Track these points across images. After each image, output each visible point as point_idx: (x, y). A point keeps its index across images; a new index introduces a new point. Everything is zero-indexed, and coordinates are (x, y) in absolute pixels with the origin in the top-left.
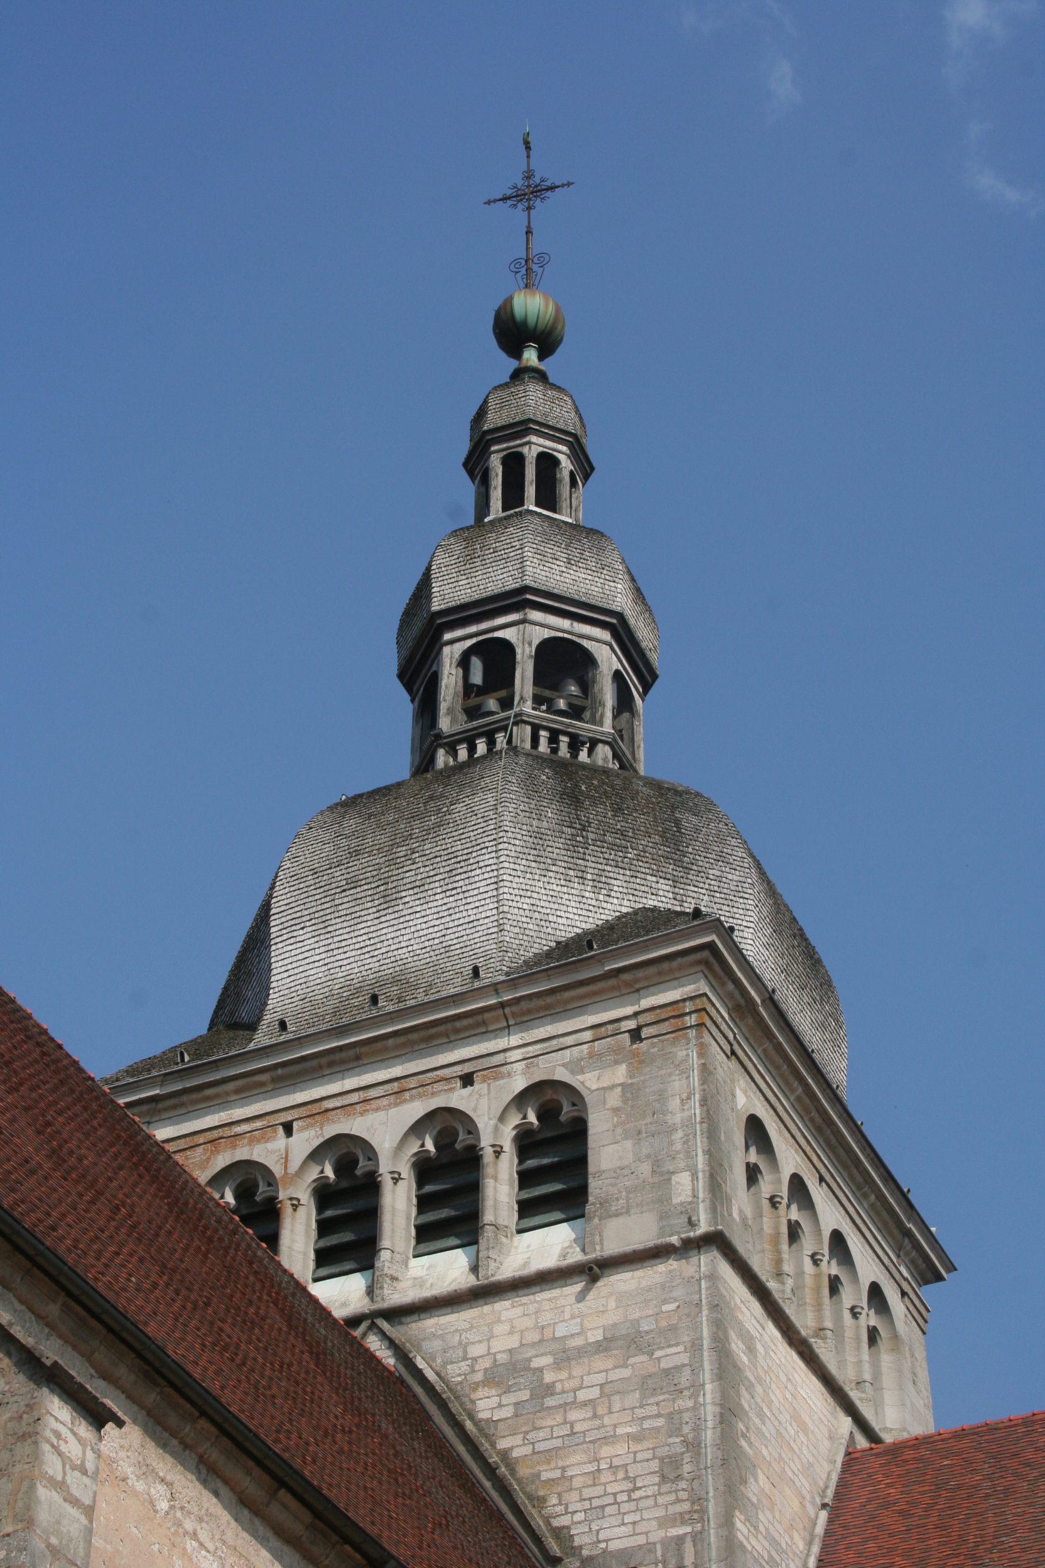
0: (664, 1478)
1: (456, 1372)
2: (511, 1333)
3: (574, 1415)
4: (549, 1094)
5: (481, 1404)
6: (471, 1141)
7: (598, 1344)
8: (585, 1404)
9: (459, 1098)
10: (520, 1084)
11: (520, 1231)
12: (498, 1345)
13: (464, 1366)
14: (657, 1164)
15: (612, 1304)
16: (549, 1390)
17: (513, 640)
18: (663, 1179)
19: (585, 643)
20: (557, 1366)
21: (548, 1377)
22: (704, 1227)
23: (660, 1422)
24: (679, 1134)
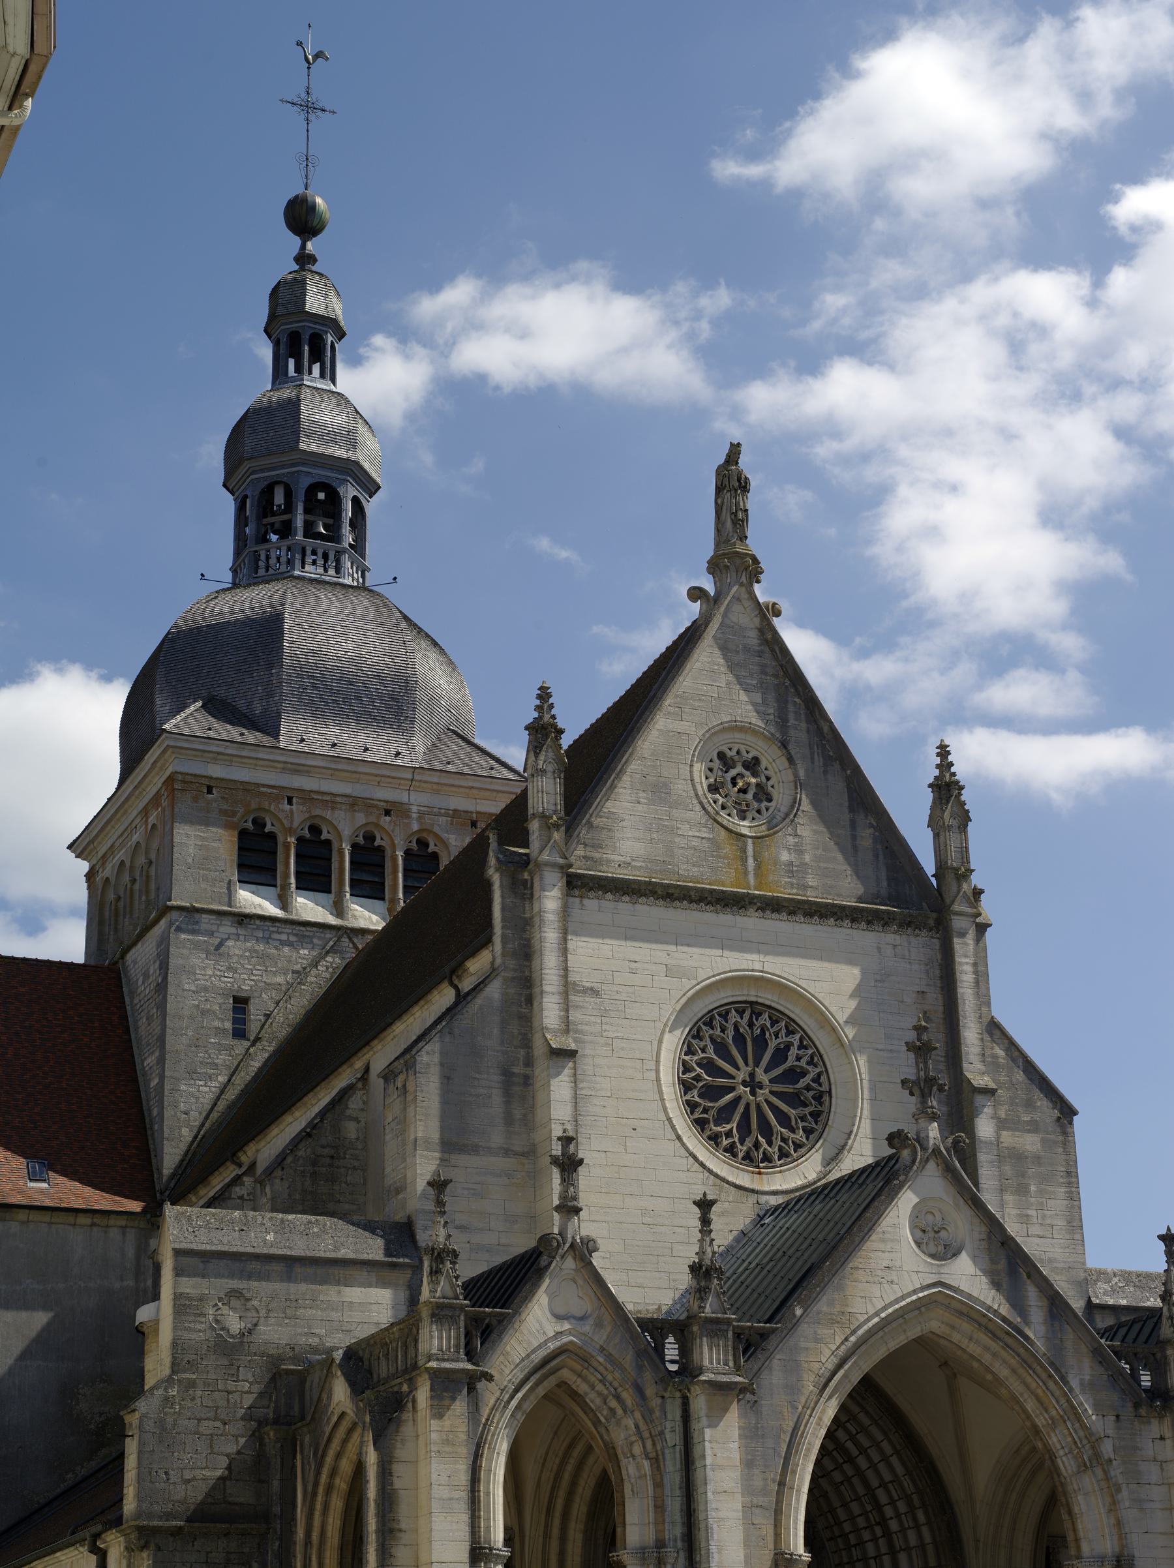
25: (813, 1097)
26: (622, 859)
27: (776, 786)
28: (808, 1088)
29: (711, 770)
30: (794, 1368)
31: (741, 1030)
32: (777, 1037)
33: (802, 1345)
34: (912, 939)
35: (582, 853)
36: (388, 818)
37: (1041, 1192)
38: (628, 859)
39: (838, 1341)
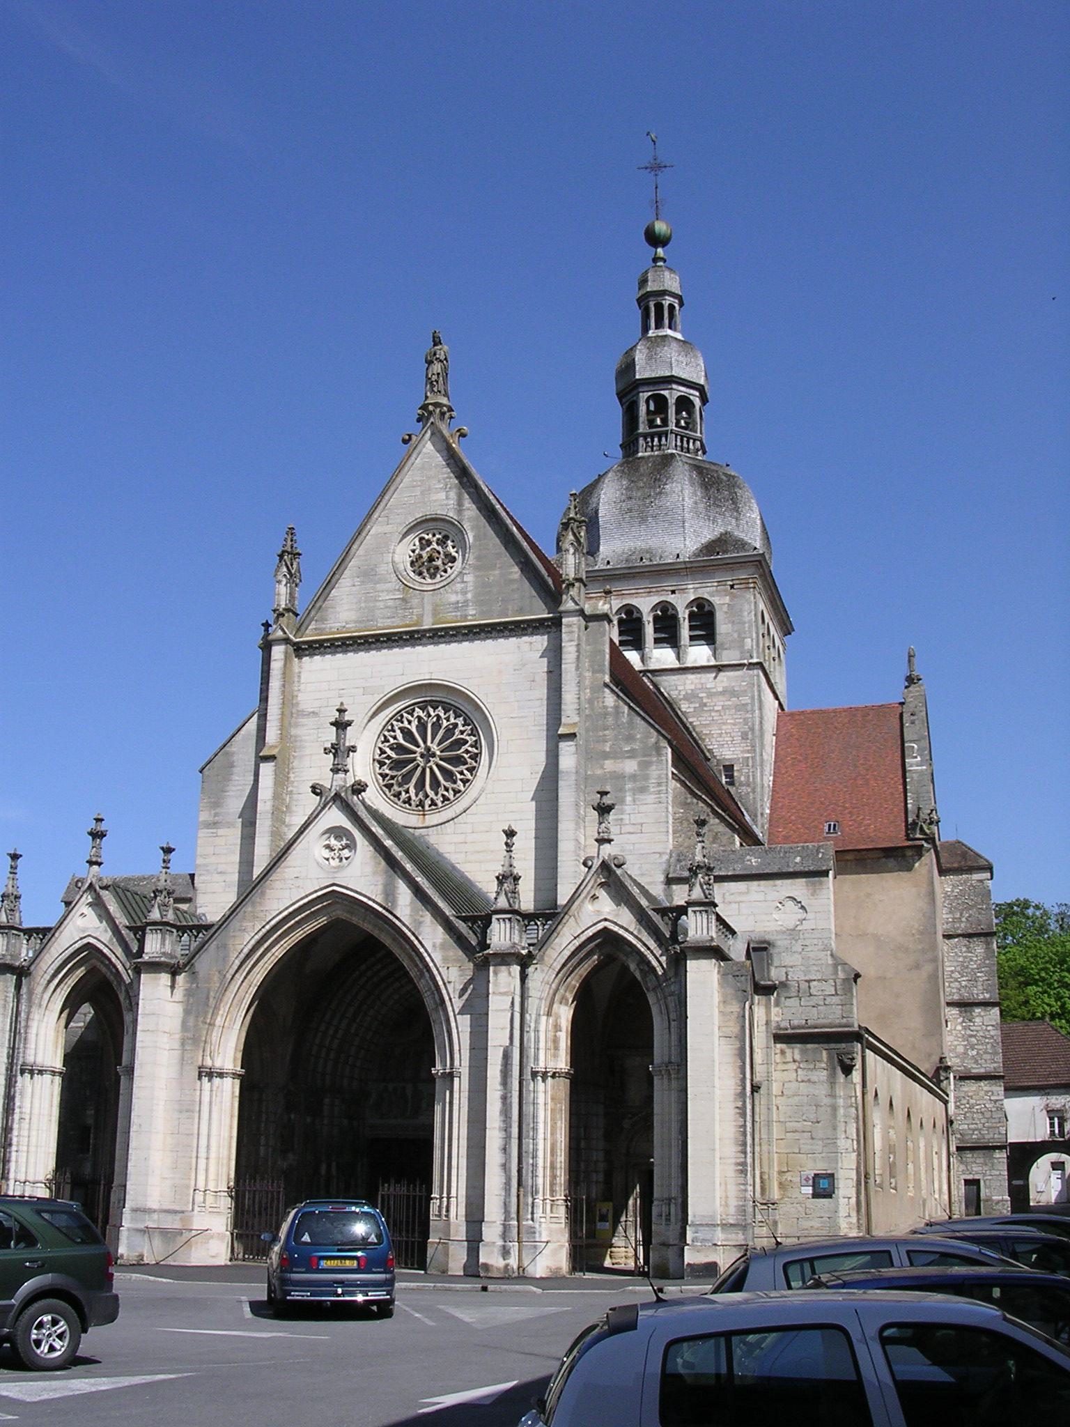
0: (743, 739)
1: (674, 694)
2: (692, 683)
3: (713, 714)
5: (682, 706)
6: (674, 612)
7: (721, 692)
9: (671, 598)
13: (677, 692)
15: (725, 680)
16: (705, 705)
17: (668, 396)
18: (742, 640)
19: (691, 397)
20: (708, 697)
21: (705, 701)
22: (755, 660)
23: (741, 720)
24: (747, 625)
33: (231, 934)
36: (673, 595)
38: (344, 624)
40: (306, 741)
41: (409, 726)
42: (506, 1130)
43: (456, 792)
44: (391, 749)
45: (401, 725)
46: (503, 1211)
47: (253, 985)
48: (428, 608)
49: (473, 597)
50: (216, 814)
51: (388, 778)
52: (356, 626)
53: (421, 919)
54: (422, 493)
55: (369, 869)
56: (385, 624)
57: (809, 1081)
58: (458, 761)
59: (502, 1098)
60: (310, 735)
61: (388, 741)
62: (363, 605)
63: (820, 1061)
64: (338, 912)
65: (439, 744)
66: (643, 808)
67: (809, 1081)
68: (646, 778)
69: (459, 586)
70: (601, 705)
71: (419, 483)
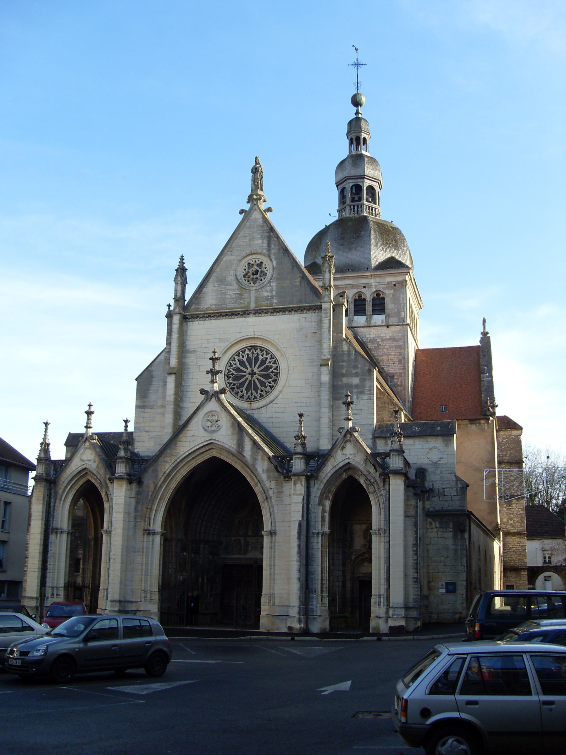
0: (399, 363)
1: (364, 339)
2: (374, 334)
3: (384, 350)
4: (379, 292)
5: (369, 345)
6: (365, 297)
7: (388, 339)
8: (386, 348)
9: (363, 290)
10: (374, 290)
11: (373, 315)
12: (371, 336)
13: (366, 338)
14: (398, 310)
15: (391, 332)
16: (380, 345)
20: (381, 341)
21: (380, 343)
23: (399, 353)
24: (402, 305)
25: (274, 375)
26: (207, 306)
27: (242, 272)
28: (272, 372)
29: (245, 270)
30: (156, 471)
31: (250, 356)
32: (263, 356)
34: (313, 314)
35: (194, 307)
37: (357, 398)
39: (173, 462)
40: (190, 365)
41: (242, 358)
42: (300, 562)
43: (267, 392)
44: (233, 370)
45: (238, 358)
46: (299, 600)
47: (171, 489)
48: (253, 299)
49: (276, 294)
50: (144, 402)
51: (232, 384)
52: (216, 308)
53: (256, 457)
54: (250, 240)
55: (230, 432)
56: (230, 306)
57: (443, 537)
58: (267, 377)
59: (298, 546)
60: (192, 362)
61: (232, 366)
62: (219, 296)
63: (449, 528)
64: (214, 453)
65: (258, 368)
66: (362, 402)
67: (443, 537)
68: (364, 387)
69: (269, 288)
70: (341, 350)
71: (248, 235)
